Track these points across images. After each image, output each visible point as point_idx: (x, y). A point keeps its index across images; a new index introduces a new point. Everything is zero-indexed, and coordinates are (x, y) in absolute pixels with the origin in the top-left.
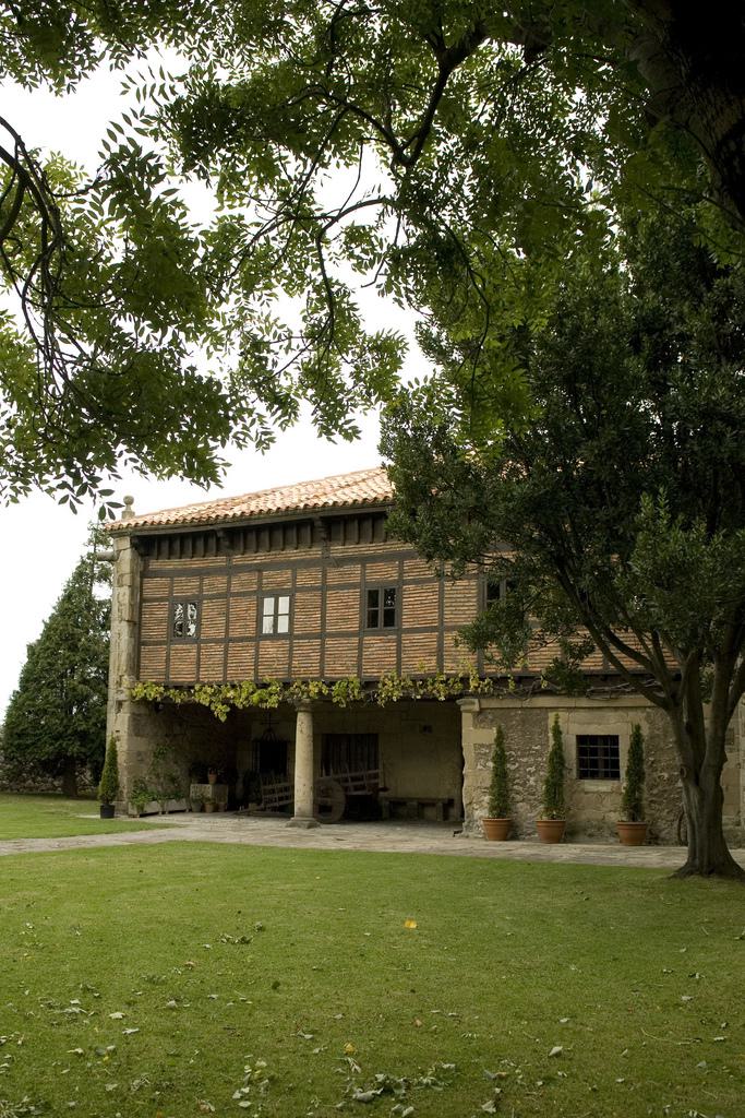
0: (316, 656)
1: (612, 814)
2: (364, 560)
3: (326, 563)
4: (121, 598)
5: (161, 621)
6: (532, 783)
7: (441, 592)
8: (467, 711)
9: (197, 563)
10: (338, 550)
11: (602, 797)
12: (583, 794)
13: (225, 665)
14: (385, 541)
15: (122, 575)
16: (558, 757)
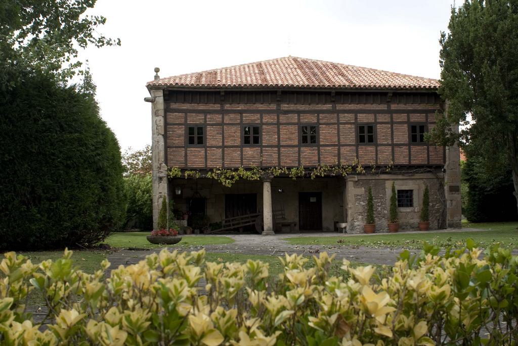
1: (411, 220)
2: (299, 112)
4: (158, 123)
5: (180, 136)
8: (350, 181)
9: (202, 107)
10: (285, 107)
12: (400, 213)
14: (310, 104)
15: (158, 110)
16: (393, 199)
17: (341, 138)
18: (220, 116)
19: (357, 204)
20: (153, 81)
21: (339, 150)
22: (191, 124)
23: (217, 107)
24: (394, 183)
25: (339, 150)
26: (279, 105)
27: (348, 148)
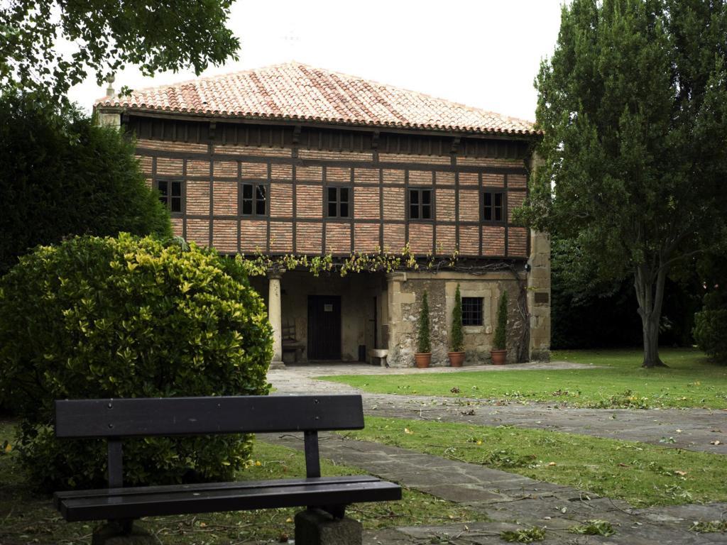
0: (289, 235)
1: (480, 347)
2: (325, 164)
3: (295, 162)
6: (436, 329)
7: (381, 195)
9: (179, 148)
10: (304, 153)
11: (480, 336)
13: (211, 238)
14: (341, 151)
16: (456, 311)
17: (385, 209)
18: (208, 165)
19: (404, 319)
20: (106, 98)
21: (381, 229)
22: (161, 176)
23: (202, 148)
24: (459, 286)
25: (381, 229)
26: (295, 151)
27: (395, 226)
